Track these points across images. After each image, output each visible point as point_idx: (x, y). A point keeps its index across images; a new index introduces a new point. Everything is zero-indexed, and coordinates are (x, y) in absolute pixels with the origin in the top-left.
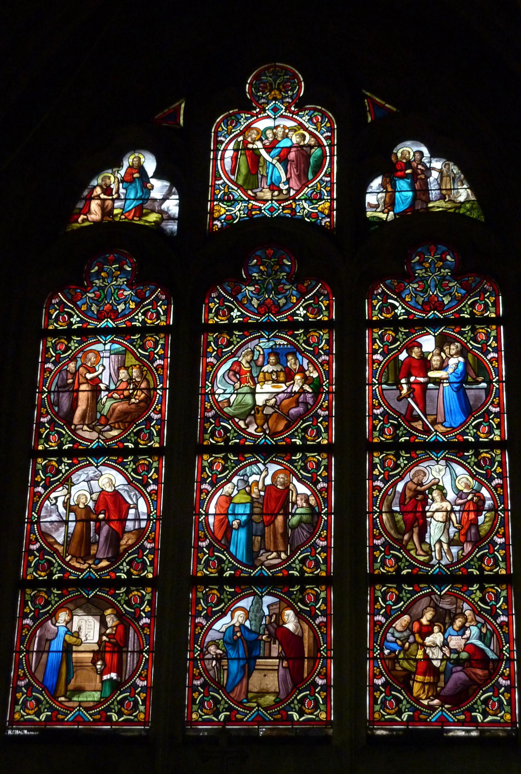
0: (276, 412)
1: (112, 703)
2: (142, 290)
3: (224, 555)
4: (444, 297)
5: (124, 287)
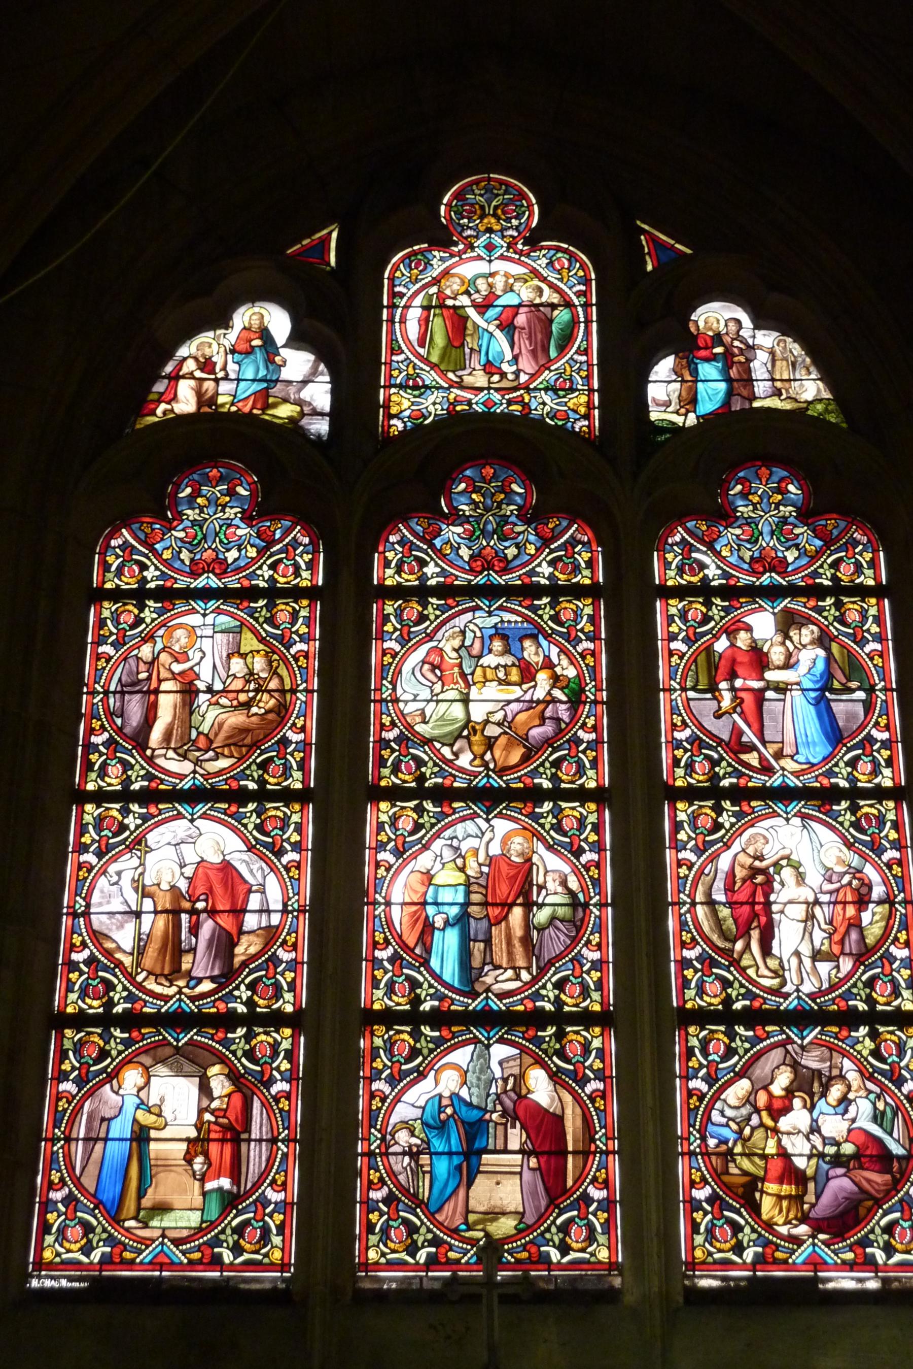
0: (505, 733)
1: (223, 1231)
2: (269, 527)
3: (420, 973)
4: (787, 549)
5: (237, 522)
